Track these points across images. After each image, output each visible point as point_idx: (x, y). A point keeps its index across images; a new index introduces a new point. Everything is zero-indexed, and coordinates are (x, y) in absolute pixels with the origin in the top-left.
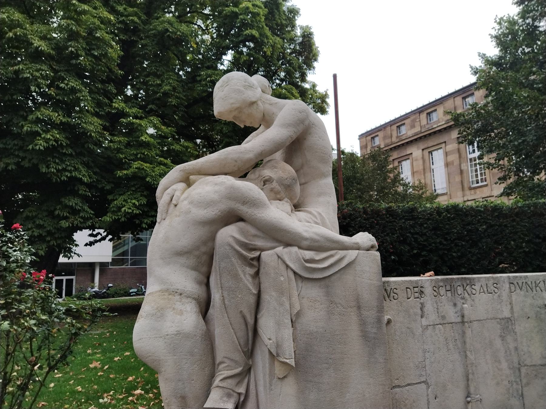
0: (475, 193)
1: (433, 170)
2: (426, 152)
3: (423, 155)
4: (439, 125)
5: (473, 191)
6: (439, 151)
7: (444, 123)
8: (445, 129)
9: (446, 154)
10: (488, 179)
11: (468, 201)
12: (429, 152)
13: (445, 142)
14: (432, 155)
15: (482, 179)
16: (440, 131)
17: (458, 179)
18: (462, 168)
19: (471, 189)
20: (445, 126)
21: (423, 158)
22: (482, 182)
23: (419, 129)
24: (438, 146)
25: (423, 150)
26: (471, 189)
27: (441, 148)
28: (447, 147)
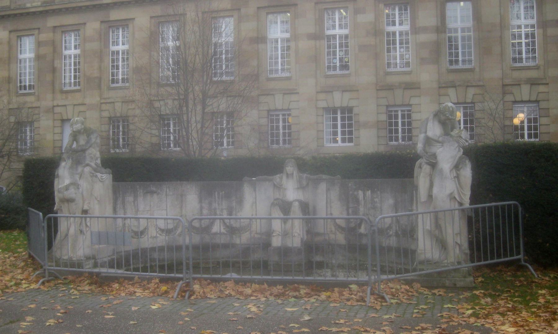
0: (67, 98)
1: (20, 60)
2: (14, 35)
3: (10, 39)
4: (34, 4)
5: (64, 94)
6: (31, 37)
7: (39, 4)
8: (41, 12)
9: (39, 44)
10: (82, 83)
11: (58, 106)
12: (18, 37)
13: (39, 29)
14: (21, 41)
15: (75, 83)
16: (34, 13)
17: (49, 77)
18: (55, 66)
19: (62, 92)
20: (41, 9)
21: (9, 42)
22: (75, 85)
23: (8, 4)
24: (28, 32)
25: (10, 32)
26: (62, 92)
27: (32, 35)
28: (41, 35)
